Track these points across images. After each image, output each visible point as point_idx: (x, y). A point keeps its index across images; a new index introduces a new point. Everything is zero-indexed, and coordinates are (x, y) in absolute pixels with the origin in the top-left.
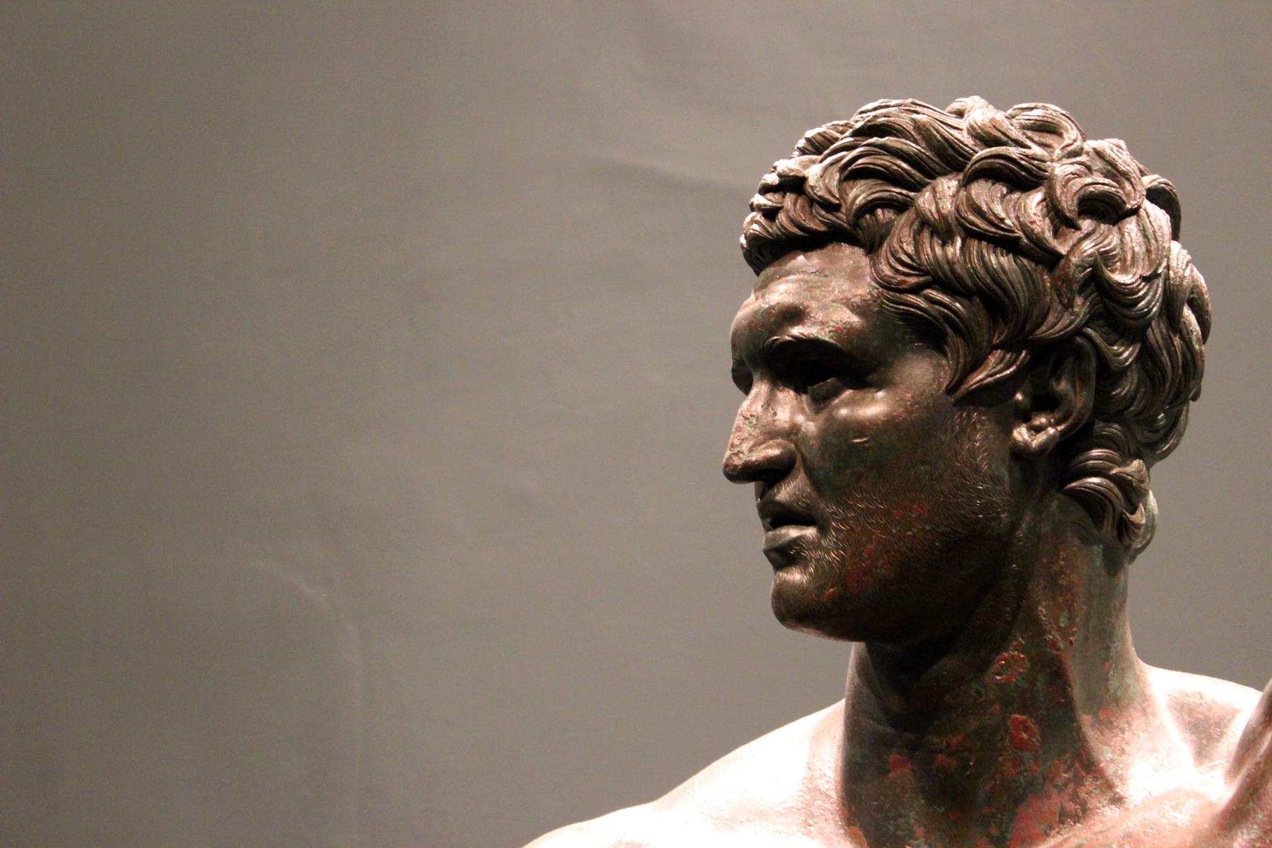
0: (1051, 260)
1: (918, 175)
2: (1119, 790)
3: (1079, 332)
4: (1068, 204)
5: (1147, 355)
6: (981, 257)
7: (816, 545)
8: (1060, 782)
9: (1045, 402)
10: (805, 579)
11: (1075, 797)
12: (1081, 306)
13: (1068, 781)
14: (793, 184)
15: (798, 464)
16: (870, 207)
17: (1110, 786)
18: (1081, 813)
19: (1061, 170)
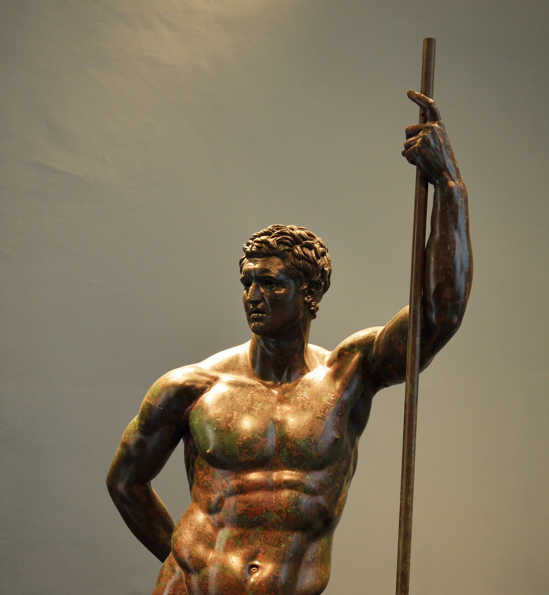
1: (293, 245)
2: (309, 369)
3: (318, 280)
4: (319, 254)
6: (305, 263)
7: (266, 318)
8: (300, 367)
9: (310, 293)
11: (302, 370)
12: (320, 275)
13: (302, 367)
17: (308, 368)
18: (303, 374)
19: (317, 246)
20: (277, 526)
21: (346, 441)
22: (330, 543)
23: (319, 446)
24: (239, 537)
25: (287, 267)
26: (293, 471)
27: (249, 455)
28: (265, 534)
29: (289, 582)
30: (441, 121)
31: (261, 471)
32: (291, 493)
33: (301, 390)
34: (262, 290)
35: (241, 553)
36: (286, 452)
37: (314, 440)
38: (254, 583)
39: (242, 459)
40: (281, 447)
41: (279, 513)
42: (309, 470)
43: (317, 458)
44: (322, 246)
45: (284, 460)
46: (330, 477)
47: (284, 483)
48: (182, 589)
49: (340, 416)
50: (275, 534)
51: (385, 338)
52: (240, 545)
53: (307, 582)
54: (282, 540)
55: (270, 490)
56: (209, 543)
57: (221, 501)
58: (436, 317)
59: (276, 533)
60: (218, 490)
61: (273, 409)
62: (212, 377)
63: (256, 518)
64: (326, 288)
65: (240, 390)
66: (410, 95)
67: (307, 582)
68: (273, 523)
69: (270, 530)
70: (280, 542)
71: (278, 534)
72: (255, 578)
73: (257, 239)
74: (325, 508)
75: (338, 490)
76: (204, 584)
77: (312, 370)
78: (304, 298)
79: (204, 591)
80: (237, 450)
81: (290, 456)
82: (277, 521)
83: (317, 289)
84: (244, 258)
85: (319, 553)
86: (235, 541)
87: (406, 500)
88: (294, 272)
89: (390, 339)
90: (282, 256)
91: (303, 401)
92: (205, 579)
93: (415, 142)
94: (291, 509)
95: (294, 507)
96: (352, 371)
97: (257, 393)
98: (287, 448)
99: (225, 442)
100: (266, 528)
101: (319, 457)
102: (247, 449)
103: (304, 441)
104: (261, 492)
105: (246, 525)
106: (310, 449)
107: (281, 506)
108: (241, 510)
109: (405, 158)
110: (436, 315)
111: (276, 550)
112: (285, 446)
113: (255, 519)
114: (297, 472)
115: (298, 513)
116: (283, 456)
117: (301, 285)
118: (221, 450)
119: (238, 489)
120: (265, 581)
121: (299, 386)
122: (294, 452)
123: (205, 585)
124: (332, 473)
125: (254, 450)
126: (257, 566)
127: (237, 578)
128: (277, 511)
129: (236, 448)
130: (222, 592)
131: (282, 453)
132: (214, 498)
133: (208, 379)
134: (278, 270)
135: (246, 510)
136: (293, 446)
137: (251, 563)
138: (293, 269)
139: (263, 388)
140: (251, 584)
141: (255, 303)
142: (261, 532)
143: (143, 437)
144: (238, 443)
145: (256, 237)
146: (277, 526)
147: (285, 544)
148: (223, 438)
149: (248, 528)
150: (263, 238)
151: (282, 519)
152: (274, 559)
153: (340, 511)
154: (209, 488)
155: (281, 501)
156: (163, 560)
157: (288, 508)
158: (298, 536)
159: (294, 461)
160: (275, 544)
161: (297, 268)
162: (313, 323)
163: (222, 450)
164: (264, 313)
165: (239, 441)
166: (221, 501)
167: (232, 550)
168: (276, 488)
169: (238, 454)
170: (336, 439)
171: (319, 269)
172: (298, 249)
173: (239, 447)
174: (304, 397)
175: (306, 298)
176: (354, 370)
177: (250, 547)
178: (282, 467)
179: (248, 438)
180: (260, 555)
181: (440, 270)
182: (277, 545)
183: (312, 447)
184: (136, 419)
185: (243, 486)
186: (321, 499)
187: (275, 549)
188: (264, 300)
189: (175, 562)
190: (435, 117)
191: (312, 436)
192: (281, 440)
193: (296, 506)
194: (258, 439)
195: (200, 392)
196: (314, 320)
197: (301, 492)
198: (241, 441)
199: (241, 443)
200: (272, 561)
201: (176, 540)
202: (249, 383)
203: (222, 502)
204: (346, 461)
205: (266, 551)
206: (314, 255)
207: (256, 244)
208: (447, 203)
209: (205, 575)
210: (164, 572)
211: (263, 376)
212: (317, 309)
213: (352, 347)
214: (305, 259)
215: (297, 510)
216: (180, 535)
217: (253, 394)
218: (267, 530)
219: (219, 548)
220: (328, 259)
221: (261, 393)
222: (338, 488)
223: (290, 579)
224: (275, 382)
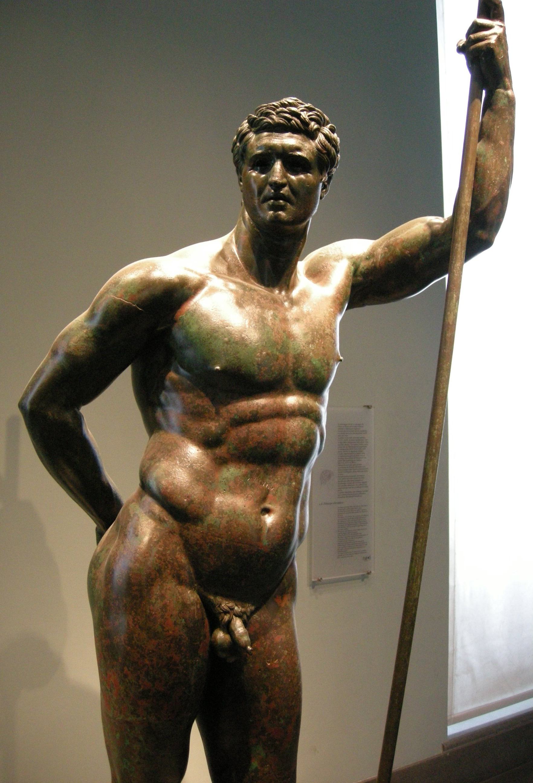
14: (298, 115)
15: (288, 185)
24: (249, 475)
35: (251, 495)
36: (301, 373)
38: (269, 530)
52: (250, 485)
54: (292, 477)
56: (211, 484)
57: (227, 431)
60: (222, 418)
69: (280, 466)
76: (209, 535)
88: (324, 157)
90: (311, 135)
98: (303, 367)
99: (242, 357)
103: (319, 360)
104: (276, 419)
107: (296, 438)
108: (254, 443)
112: (301, 365)
116: (297, 377)
118: (236, 367)
123: (210, 536)
129: (254, 365)
136: (309, 366)
137: (262, 506)
138: (324, 154)
144: (257, 359)
148: (238, 353)
150: (293, 109)
154: (207, 415)
155: (295, 431)
157: (302, 439)
163: (238, 367)
165: (258, 357)
166: (227, 431)
176: (347, 285)
178: (294, 391)
179: (268, 354)
191: (325, 355)
192: (296, 358)
194: (277, 355)
198: (261, 357)
199: (260, 359)
203: (227, 432)
209: (211, 524)
219: (224, 490)
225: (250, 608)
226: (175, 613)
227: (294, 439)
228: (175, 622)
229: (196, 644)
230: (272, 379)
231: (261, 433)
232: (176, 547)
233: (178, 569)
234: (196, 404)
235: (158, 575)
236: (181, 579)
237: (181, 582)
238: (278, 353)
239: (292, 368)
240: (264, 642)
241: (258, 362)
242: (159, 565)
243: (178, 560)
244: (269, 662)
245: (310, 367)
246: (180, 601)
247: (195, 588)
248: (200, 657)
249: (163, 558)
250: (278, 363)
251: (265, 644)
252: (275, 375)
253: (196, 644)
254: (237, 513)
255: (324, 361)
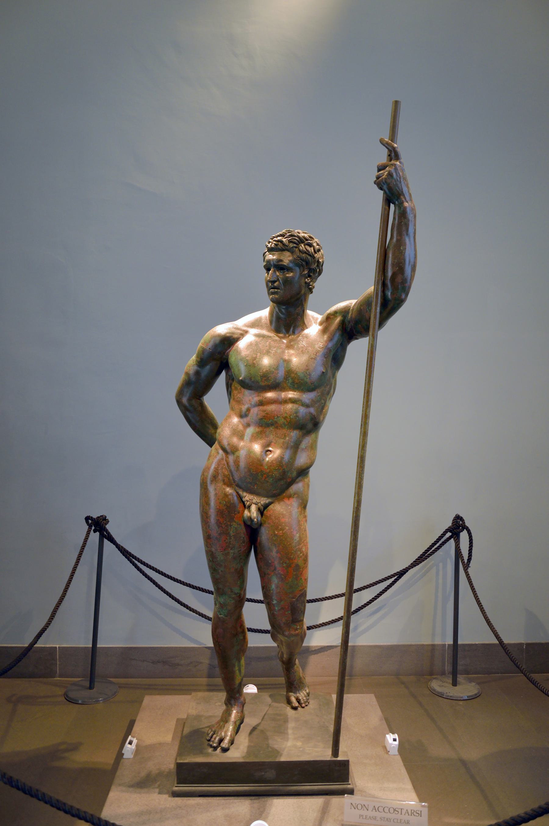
0: (314, 258)
2: (307, 327)
3: (315, 268)
4: (316, 250)
5: (320, 270)
7: (280, 292)
9: (309, 276)
10: (278, 297)
11: (303, 327)
12: (316, 264)
14: (281, 241)
16: (293, 247)
17: (306, 326)
18: (303, 330)
19: (315, 244)
20: (284, 426)
21: (330, 373)
22: (317, 438)
23: (312, 376)
24: (259, 433)
25: (295, 259)
26: (295, 392)
27: (266, 381)
28: (276, 431)
29: (290, 460)
30: (402, 160)
31: (274, 391)
32: (293, 406)
33: (301, 340)
34: (278, 274)
36: (290, 380)
37: (309, 373)
38: (268, 461)
39: (262, 384)
40: (287, 376)
41: (285, 418)
42: (305, 392)
43: (310, 384)
44: (318, 245)
45: (289, 385)
46: (318, 396)
47: (289, 400)
48: (223, 464)
49: (326, 358)
50: (282, 431)
51: (357, 308)
53: (302, 461)
54: (286, 435)
55: (280, 403)
56: (240, 436)
58: (391, 294)
59: (283, 431)
61: (283, 352)
62: (244, 331)
63: (271, 421)
64: (320, 273)
65: (262, 340)
66: (382, 141)
67: (302, 461)
68: (281, 425)
69: (279, 429)
70: (285, 436)
71: (284, 431)
72: (269, 458)
73: (275, 239)
74: (314, 416)
75: (323, 404)
77: (309, 327)
78: (305, 280)
79: (237, 466)
80: (259, 378)
81: (293, 382)
82: (284, 423)
83: (314, 274)
84: (266, 252)
85: (310, 443)
86: (257, 435)
87: (366, 412)
88: (299, 262)
89: (360, 308)
91: (302, 348)
92: (238, 458)
93: (383, 174)
94: (293, 416)
95: (295, 415)
96: (335, 329)
97: (273, 341)
99: (252, 373)
100: (277, 428)
101: (312, 384)
102: (265, 377)
103: (303, 373)
104: (274, 404)
105: (264, 425)
106: (306, 378)
107: (287, 414)
109: (376, 186)
110: (391, 293)
111: (282, 441)
112: (290, 376)
113: (270, 422)
114: (297, 392)
115: (297, 418)
116: (289, 382)
117: (304, 271)
119: (260, 403)
120: (276, 460)
121: (300, 338)
122: (296, 380)
124: (320, 394)
125: (270, 378)
126: (270, 451)
127: (258, 458)
128: (284, 417)
130: (248, 466)
131: (288, 380)
132: (244, 408)
133: (241, 332)
134: (289, 260)
135: (264, 416)
138: (298, 260)
139: (277, 338)
140: (267, 462)
141: (273, 282)
142: (274, 430)
143: (199, 369)
144: (260, 374)
145: (274, 237)
146: (284, 426)
147: (288, 438)
148: (250, 370)
149: (265, 427)
150: (279, 238)
151: (287, 422)
152: (281, 446)
153: (324, 418)
154: (241, 402)
156: (211, 446)
157: (291, 415)
158: (297, 433)
159: (296, 386)
160: (282, 438)
161: (301, 259)
162: (311, 296)
164: (279, 289)
167: (255, 441)
168: (284, 402)
169: (260, 381)
170: (323, 372)
171: (315, 261)
172: (302, 247)
173: (260, 376)
174: (303, 345)
175: (306, 280)
176: (336, 328)
177: (266, 439)
179: (267, 371)
180: (273, 444)
181: (395, 263)
182: (284, 438)
183: (307, 377)
184: (194, 357)
185: (263, 401)
186: (312, 410)
187: (282, 440)
188: (279, 281)
189: (219, 448)
190: (397, 157)
191: (307, 370)
193: (296, 414)
195: (236, 340)
196: (311, 294)
197: (300, 405)
198: (262, 372)
199: (262, 373)
200: (280, 448)
201: (219, 434)
202: (267, 335)
204: (329, 386)
205: (276, 441)
206: (313, 251)
207: (274, 242)
208: (402, 218)
210: (212, 453)
211: (277, 331)
212: (314, 287)
213: (335, 313)
214: (305, 253)
215: (297, 417)
216: (222, 431)
217: (270, 342)
218: (277, 429)
220: (322, 254)
221: (275, 342)
222: (323, 404)
223: (291, 459)
224: (285, 335)
225: (264, 501)
226: (221, 498)
227: (286, 415)
228: (220, 502)
229: (232, 515)
230: (269, 384)
231: (265, 411)
232: (223, 466)
233: (223, 477)
234: (238, 397)
235: (214, 479)
236: (225, 482)
237: (225, 484)
238: (273, 370)
239: (285, 378)
240: (274, 521)
241: (260, 375)
242: (215, 474)
243: (224, 472)
244: (277, 531)
245: (296, 377)
246: (224, 492)
247: (233, 487)
248: (235, 522)
249: (217, 471)
250: (273, 375)
251: (275, 521)
252: (271, 382)
253: (232, 515)
254: (250, 451)
255: (307, 373)
